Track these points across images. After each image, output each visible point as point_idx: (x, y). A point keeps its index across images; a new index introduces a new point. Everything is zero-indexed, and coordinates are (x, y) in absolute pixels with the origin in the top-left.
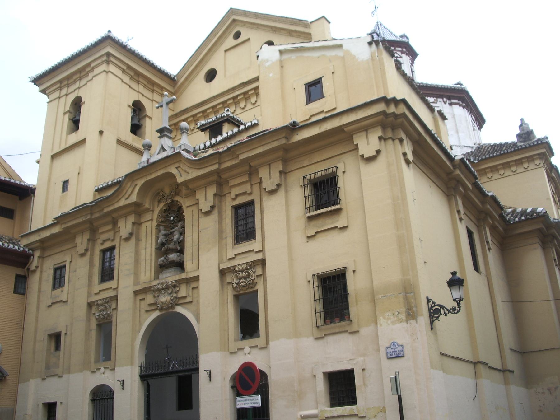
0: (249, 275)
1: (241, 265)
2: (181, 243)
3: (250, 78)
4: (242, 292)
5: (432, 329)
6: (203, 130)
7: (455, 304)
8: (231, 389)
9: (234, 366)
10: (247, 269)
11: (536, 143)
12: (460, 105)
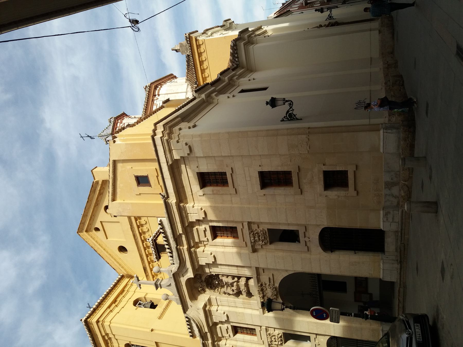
0: (257, 233)
1: (250, 238)
2: (233, 277)
3: (128, 223)
4: (268, 239)
5: (301, 119)
6: (160, 258)
7: (287, 103)
8: (333, 253)
9: (317, 249)
11: (188, 42)
12: (160, 89)
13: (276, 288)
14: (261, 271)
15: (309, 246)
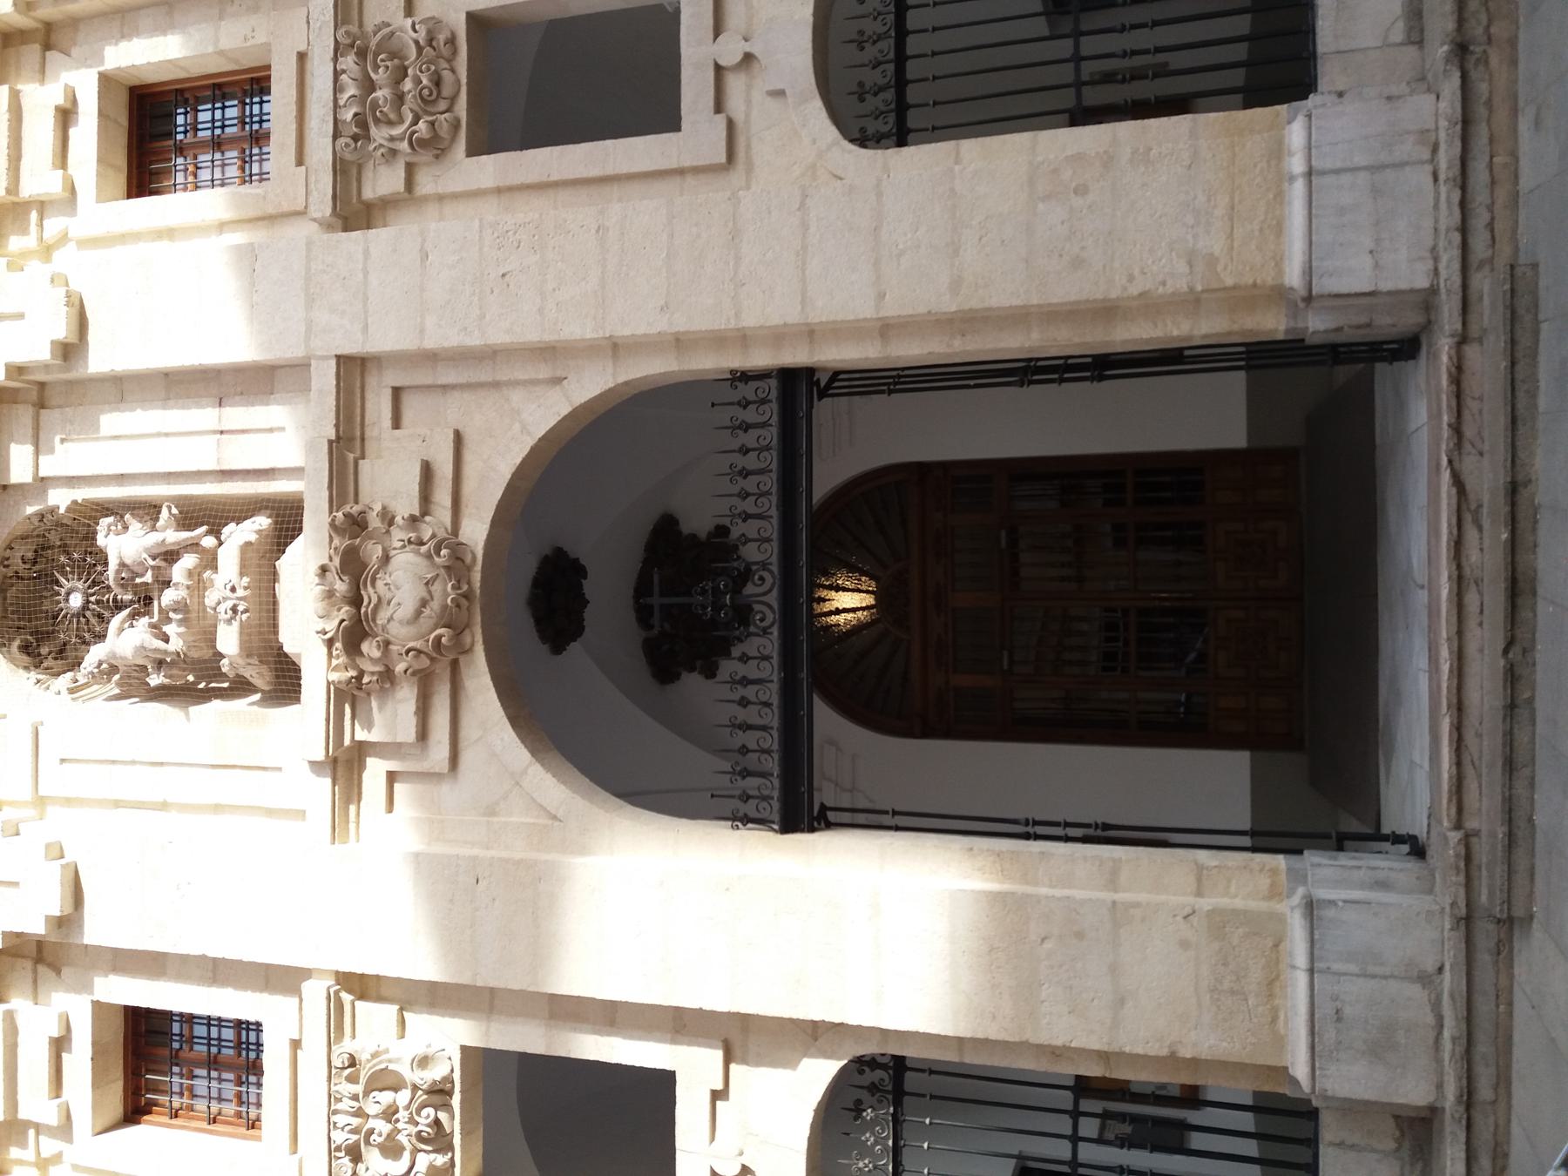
1: (337, 88)
10: (362, 54)
14: (379, 407)
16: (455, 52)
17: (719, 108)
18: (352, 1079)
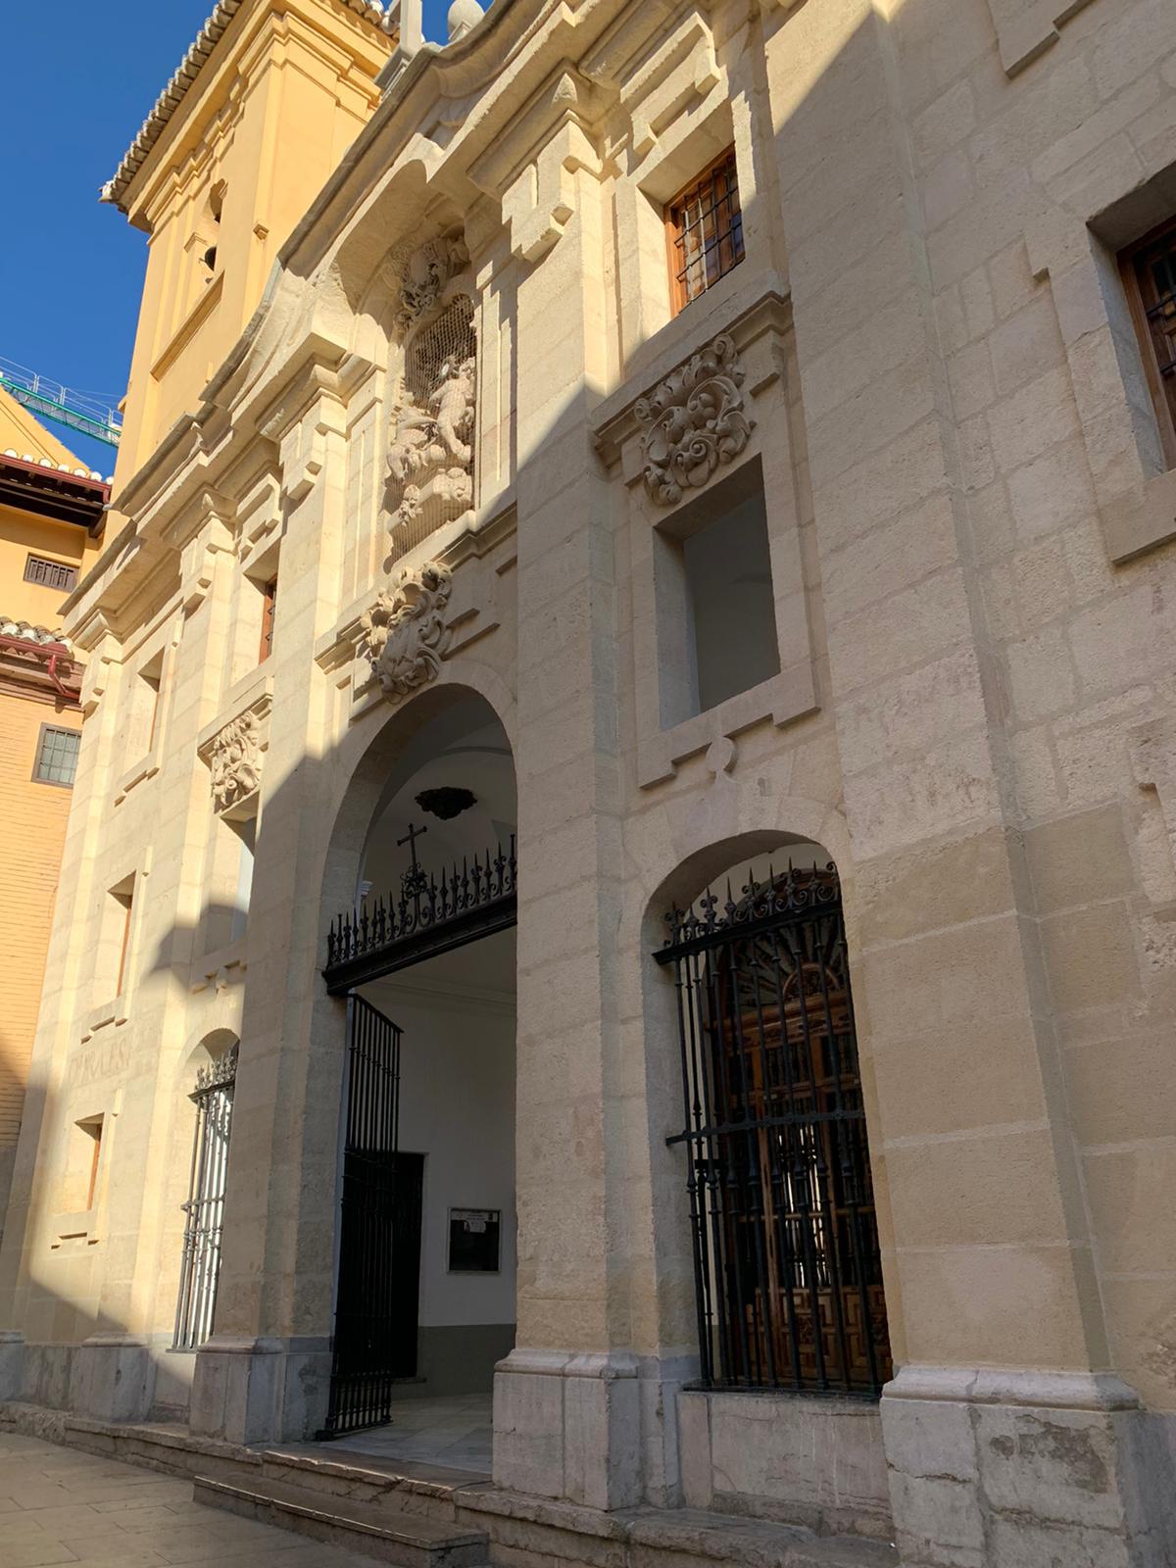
1: (676, 370)
2: (466, 434)
10: (706, 373)
13: (425, 670)
15: (678, 785)
16: (728, 462)
17: (677, 763)
18: (243, 730)
